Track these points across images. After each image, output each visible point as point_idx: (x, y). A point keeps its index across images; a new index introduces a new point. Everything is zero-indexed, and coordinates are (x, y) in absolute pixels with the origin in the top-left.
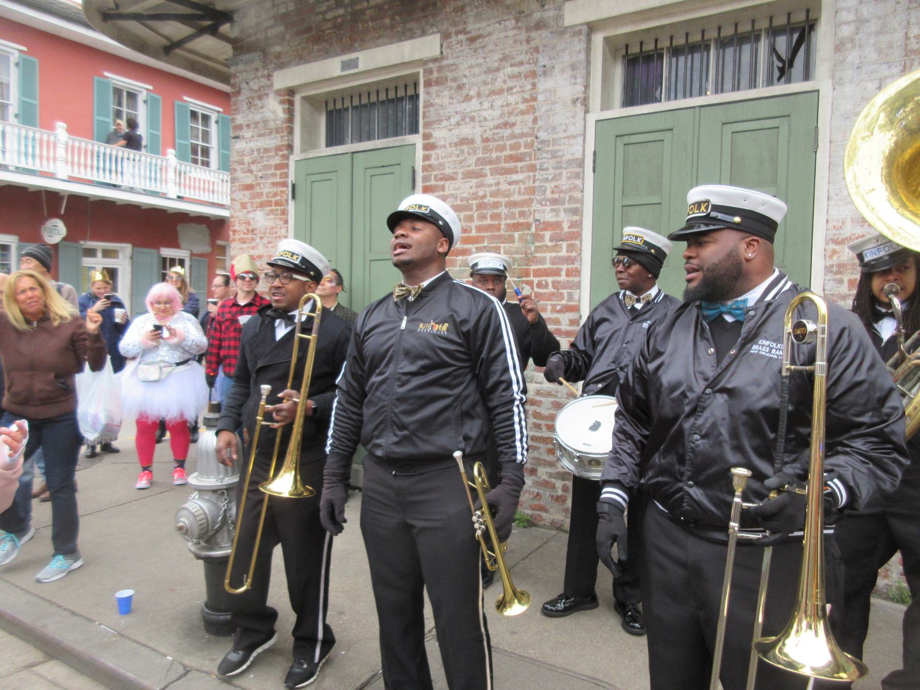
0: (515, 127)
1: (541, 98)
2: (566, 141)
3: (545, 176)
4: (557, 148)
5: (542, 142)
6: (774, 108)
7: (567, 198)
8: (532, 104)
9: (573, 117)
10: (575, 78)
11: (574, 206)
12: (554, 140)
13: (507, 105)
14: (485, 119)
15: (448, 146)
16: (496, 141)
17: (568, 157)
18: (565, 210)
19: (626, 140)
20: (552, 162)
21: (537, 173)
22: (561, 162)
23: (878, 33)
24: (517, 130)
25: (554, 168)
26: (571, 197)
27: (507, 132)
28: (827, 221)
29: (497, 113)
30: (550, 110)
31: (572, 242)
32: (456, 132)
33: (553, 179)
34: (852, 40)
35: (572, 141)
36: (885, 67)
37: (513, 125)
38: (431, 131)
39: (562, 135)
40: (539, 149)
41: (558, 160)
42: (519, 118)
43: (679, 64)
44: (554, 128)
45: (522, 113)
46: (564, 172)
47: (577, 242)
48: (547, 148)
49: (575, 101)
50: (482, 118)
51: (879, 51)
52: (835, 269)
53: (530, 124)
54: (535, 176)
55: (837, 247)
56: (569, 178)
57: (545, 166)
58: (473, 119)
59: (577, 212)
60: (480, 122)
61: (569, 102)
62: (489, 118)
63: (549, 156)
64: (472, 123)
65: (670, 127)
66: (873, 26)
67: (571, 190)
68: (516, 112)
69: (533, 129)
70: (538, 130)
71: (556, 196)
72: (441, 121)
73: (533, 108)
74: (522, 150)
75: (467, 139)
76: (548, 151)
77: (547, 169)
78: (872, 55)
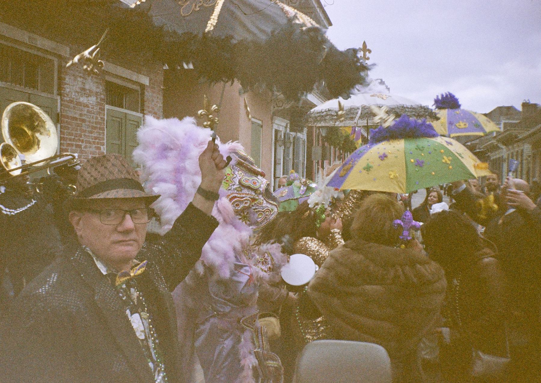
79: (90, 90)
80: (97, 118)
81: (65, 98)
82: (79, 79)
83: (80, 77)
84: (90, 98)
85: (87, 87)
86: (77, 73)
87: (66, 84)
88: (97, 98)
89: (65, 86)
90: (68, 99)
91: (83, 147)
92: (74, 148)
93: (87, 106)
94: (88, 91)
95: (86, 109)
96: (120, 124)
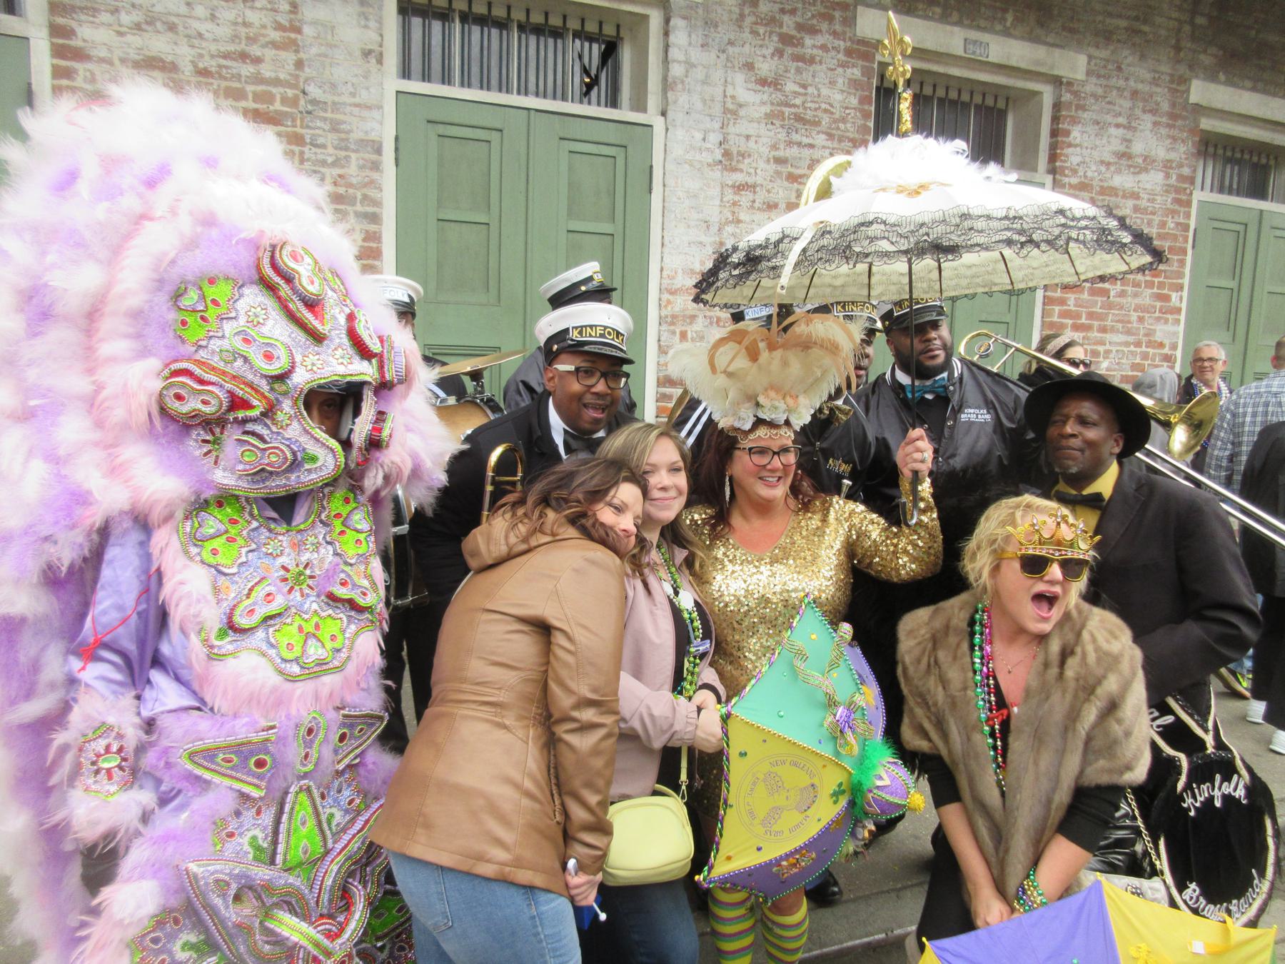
0: (262, 66)
1: (307, 30)
2: (356, 111)
3: (321, 157)
4: (339, 117)
5: (314, 102)
6: (611, 134)
7: (359, 197)
8: (293, 36)
9: (366, 77)
10: (367, 19)
11: (370, 209)
12: (334, 103)
13: (245, 24)
14: (200, 35)
15: (117, 62)
16: (226, 79)
17: (355, 136)
18: (357, 214)
19: (441, 129)
20: (331, 138)
21: (306, 149)
22: (347, 140)
23: (704, 83)
24: (267, 71)
25: (336, 148)
26: (365, 197)
27: (247, 70)
28: (662, 270)
29: (224, 31)
30: (326, 56)
31: (370, 262)
32: (134, 40)
33: (335, 164)
34: (683, 82)
35: (365, 113)
36: (708, 119)
37: (257, 61)
38: (74, 24)
39: (346, 99)
40: (309, 113)
41: (343, 136)
42: (269, 53)
43: (473, 38)
44: (333, 86)
45: (274, 45)
46: (353, 156)
47: (377, 263)
48: (322, 114)
49: (367, 54)
50: (193, 33)
51: (704, 101)
52: (669, 320)
53: (291, 68)
54: (302, 153)
55: (671, 297)
56: (361, 168)
57: (320, 141)
58: (172, 28)
59: (375, 218)
60: (188, 36)
61: (358, 53)
62: (207, 35)
63: (327, 128)
64: (170, 35)
65: (499, 126)
66: (699, 73)
67: (365, 185)
68: (263, 40)
69: (297, 77)
70: (306, 80)
71: (341, 190)
72: (95, 11)
73: (294, 42)
74: (278, 106)
75: (162, 60)
76: (325, 119)
77: (323, 146)
78: (699, 105)
79: (1146, 158)
80: (1163, 224)
81: (1066, 180)
82: (1113, 131)
83: (1118, 126)
84: (1143, 177)
85: (1138, 148)
86: (1109, 118)
87: (1070, 145)
88: (1167, 176)
89: (1070, 150)
90: (1074, 181)
91: (1112, 293)
92: (1085, 296)
93: (1135, 196)
94: (1140, 160)
95: (1130, 203)
96: (1240, 238)
